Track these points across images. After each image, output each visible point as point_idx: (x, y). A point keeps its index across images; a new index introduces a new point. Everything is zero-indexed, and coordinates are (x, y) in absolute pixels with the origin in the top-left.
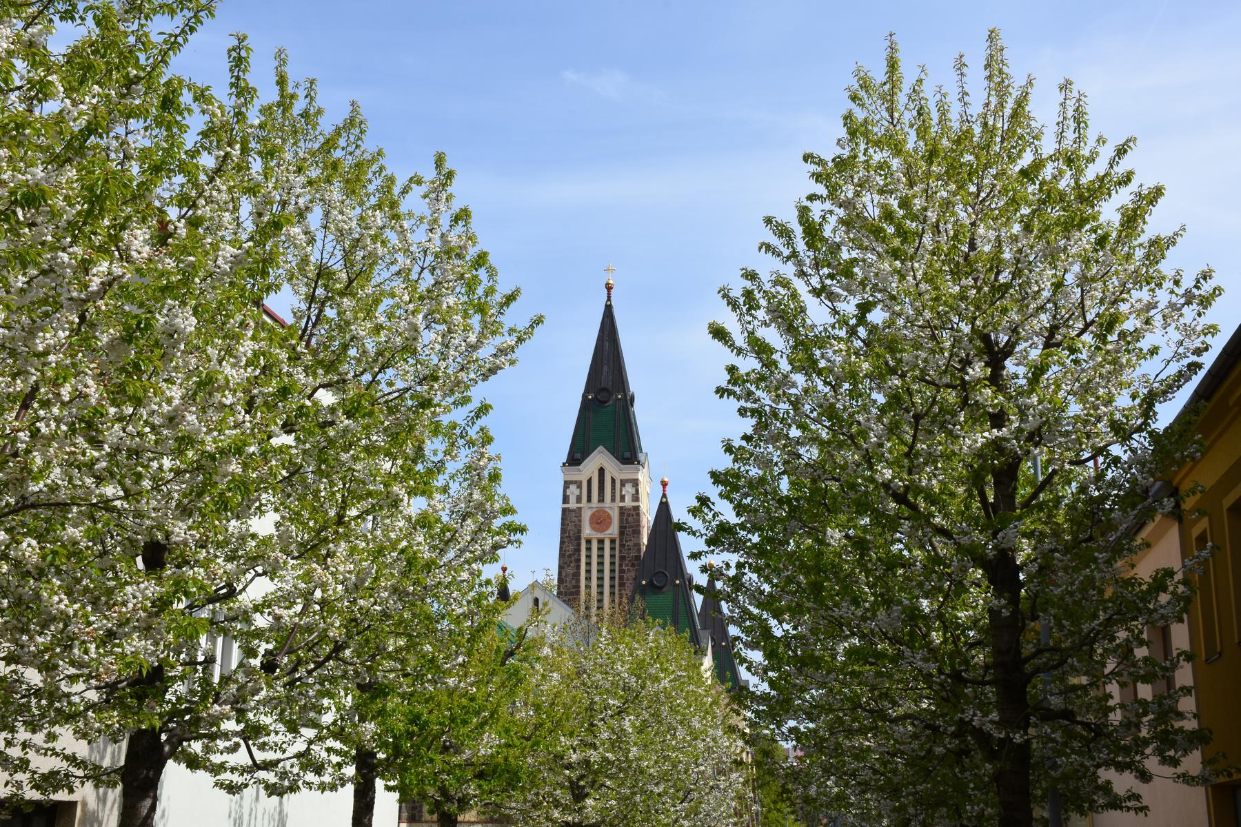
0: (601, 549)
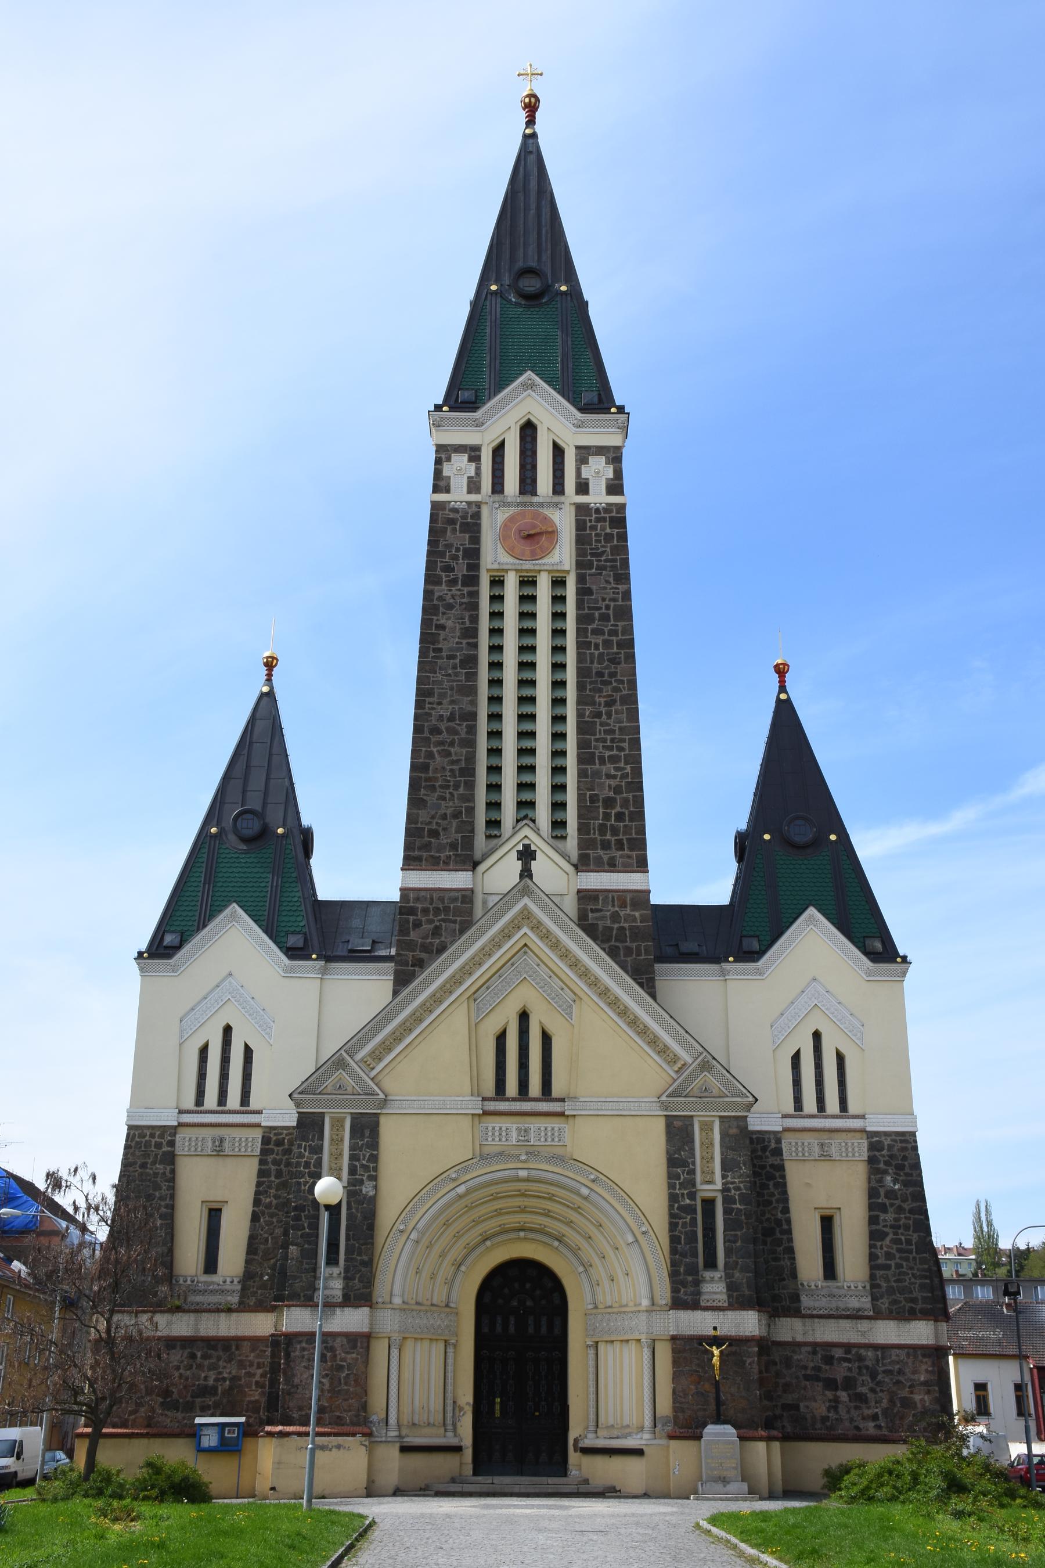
0: (528, 599)
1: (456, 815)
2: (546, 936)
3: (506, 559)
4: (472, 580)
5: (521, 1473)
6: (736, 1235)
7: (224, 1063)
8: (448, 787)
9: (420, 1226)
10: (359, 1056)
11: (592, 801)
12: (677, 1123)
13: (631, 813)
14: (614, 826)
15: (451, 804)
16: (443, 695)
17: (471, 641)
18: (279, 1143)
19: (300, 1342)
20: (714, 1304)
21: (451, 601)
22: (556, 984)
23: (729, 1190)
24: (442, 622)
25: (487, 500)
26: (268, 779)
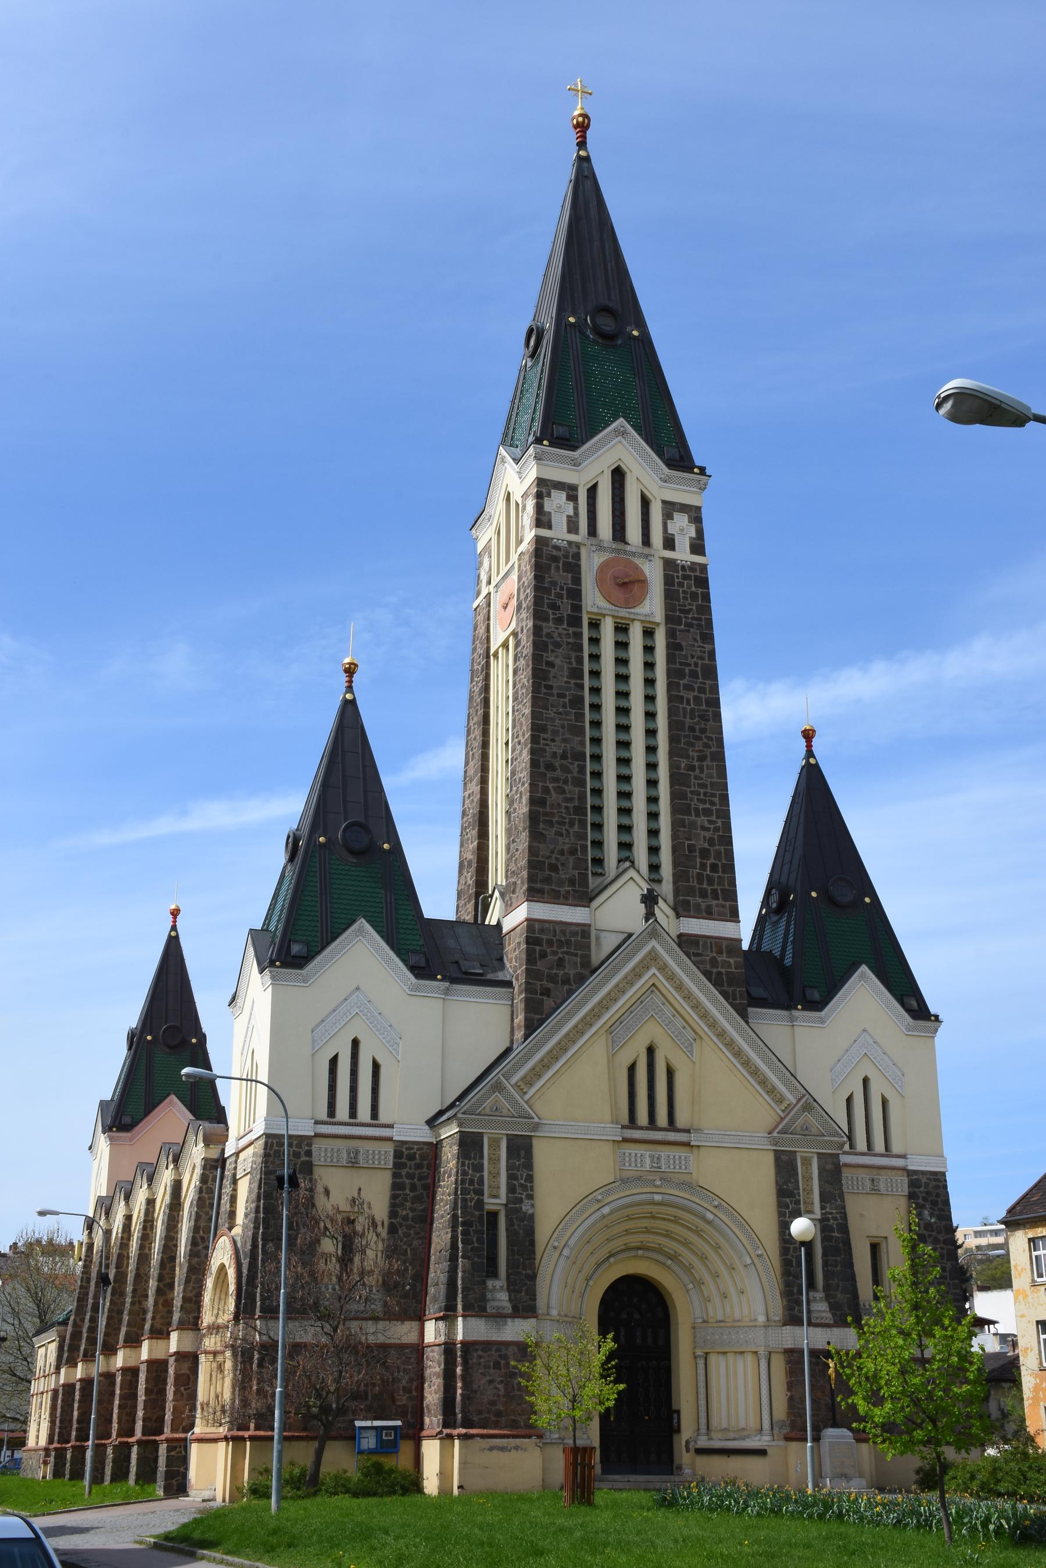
1: (573, 852)
2: (671, 977)
3: (602, 603)
4: (575, 621)
5: (635, 1472)
6: (836, 1261)
7: (350, 1076)
8: (564, 823)
9: (572, 1242)
10: (514, 1080)
11: (690, 851)
12: (784, 1158)
13: (723, 865)
14: (705, 876)
15: (567, 840)
16: (555, 733)
17: (578, 681)
18: (411, 1157)
19: (476, 1350)
20: (822, 1321)
21: (559, 639)
22: (679, 1022)
23: (828, 1220)
24: (551, 659)
25: (586, 541)
26: (365, 792)
